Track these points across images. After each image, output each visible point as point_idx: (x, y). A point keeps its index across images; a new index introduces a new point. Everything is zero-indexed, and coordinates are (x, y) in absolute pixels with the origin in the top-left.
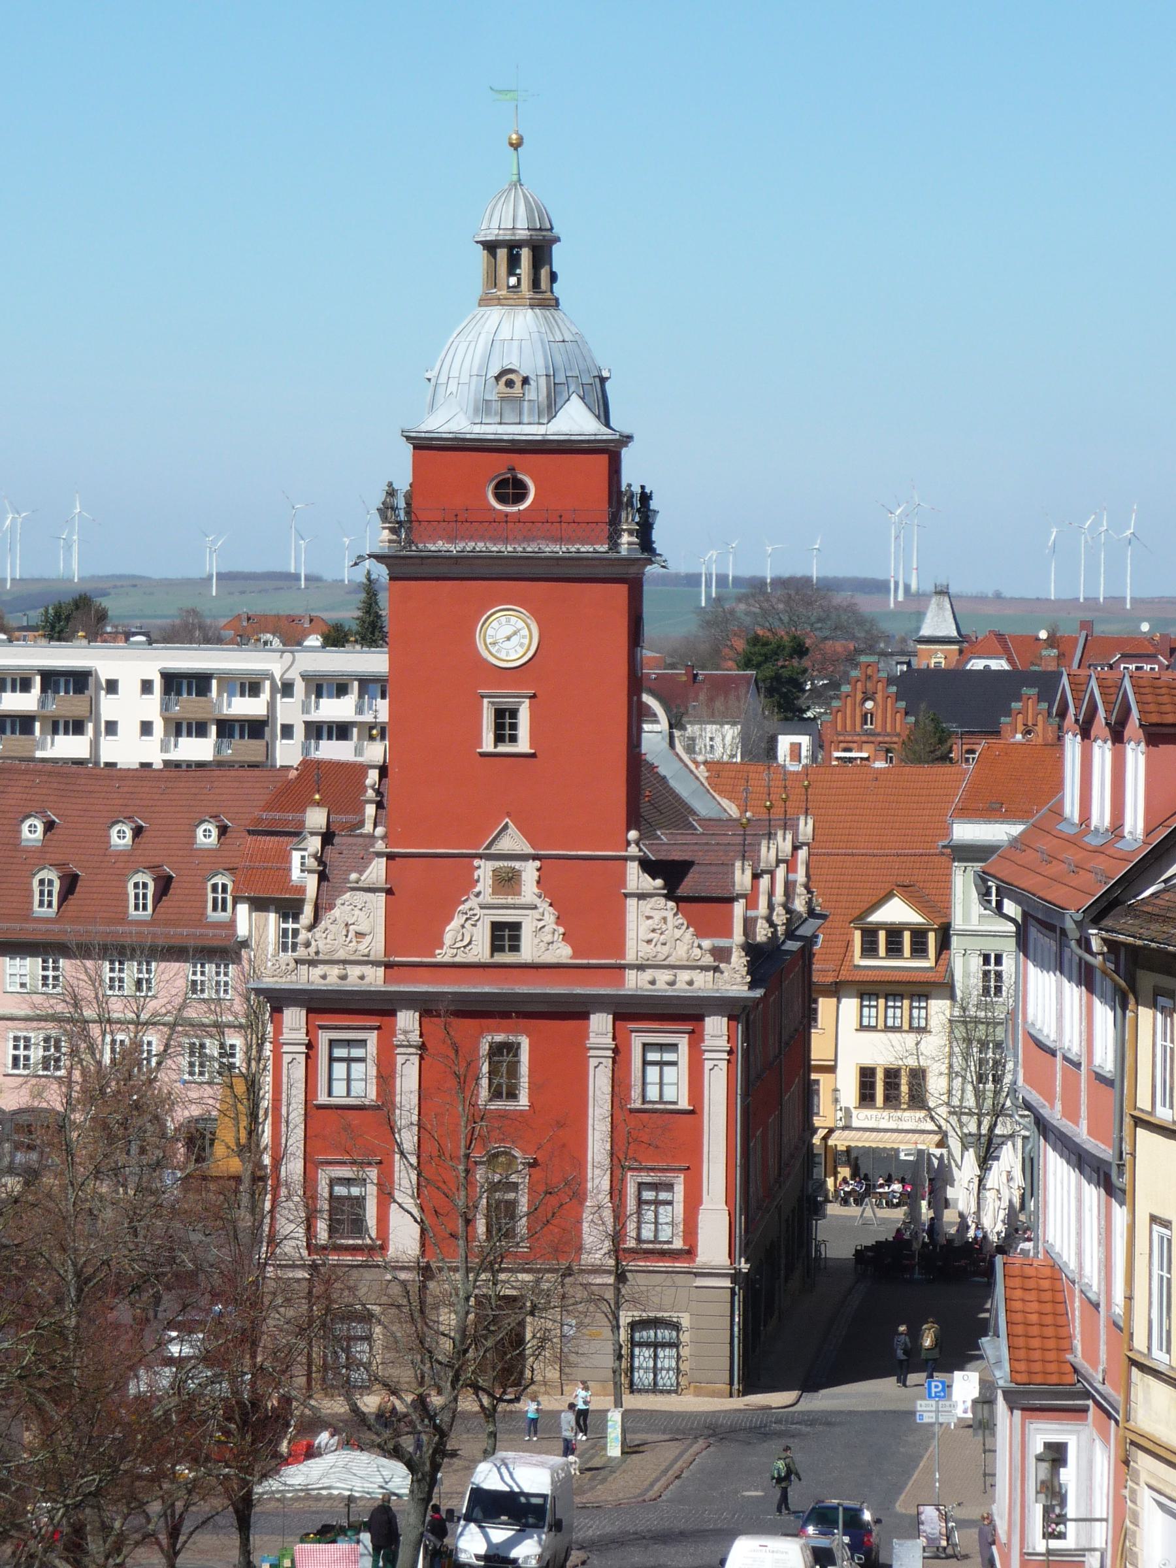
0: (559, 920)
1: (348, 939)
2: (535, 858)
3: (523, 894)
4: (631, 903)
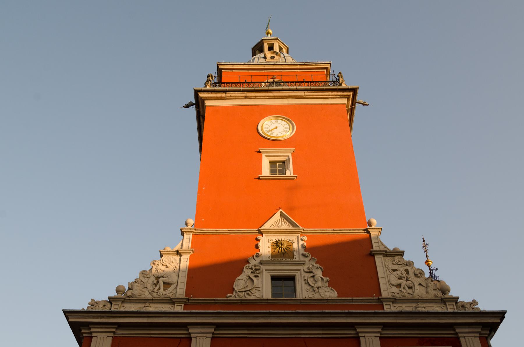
1: (158, 287)
3: (295, 257)
4: (379, 260)
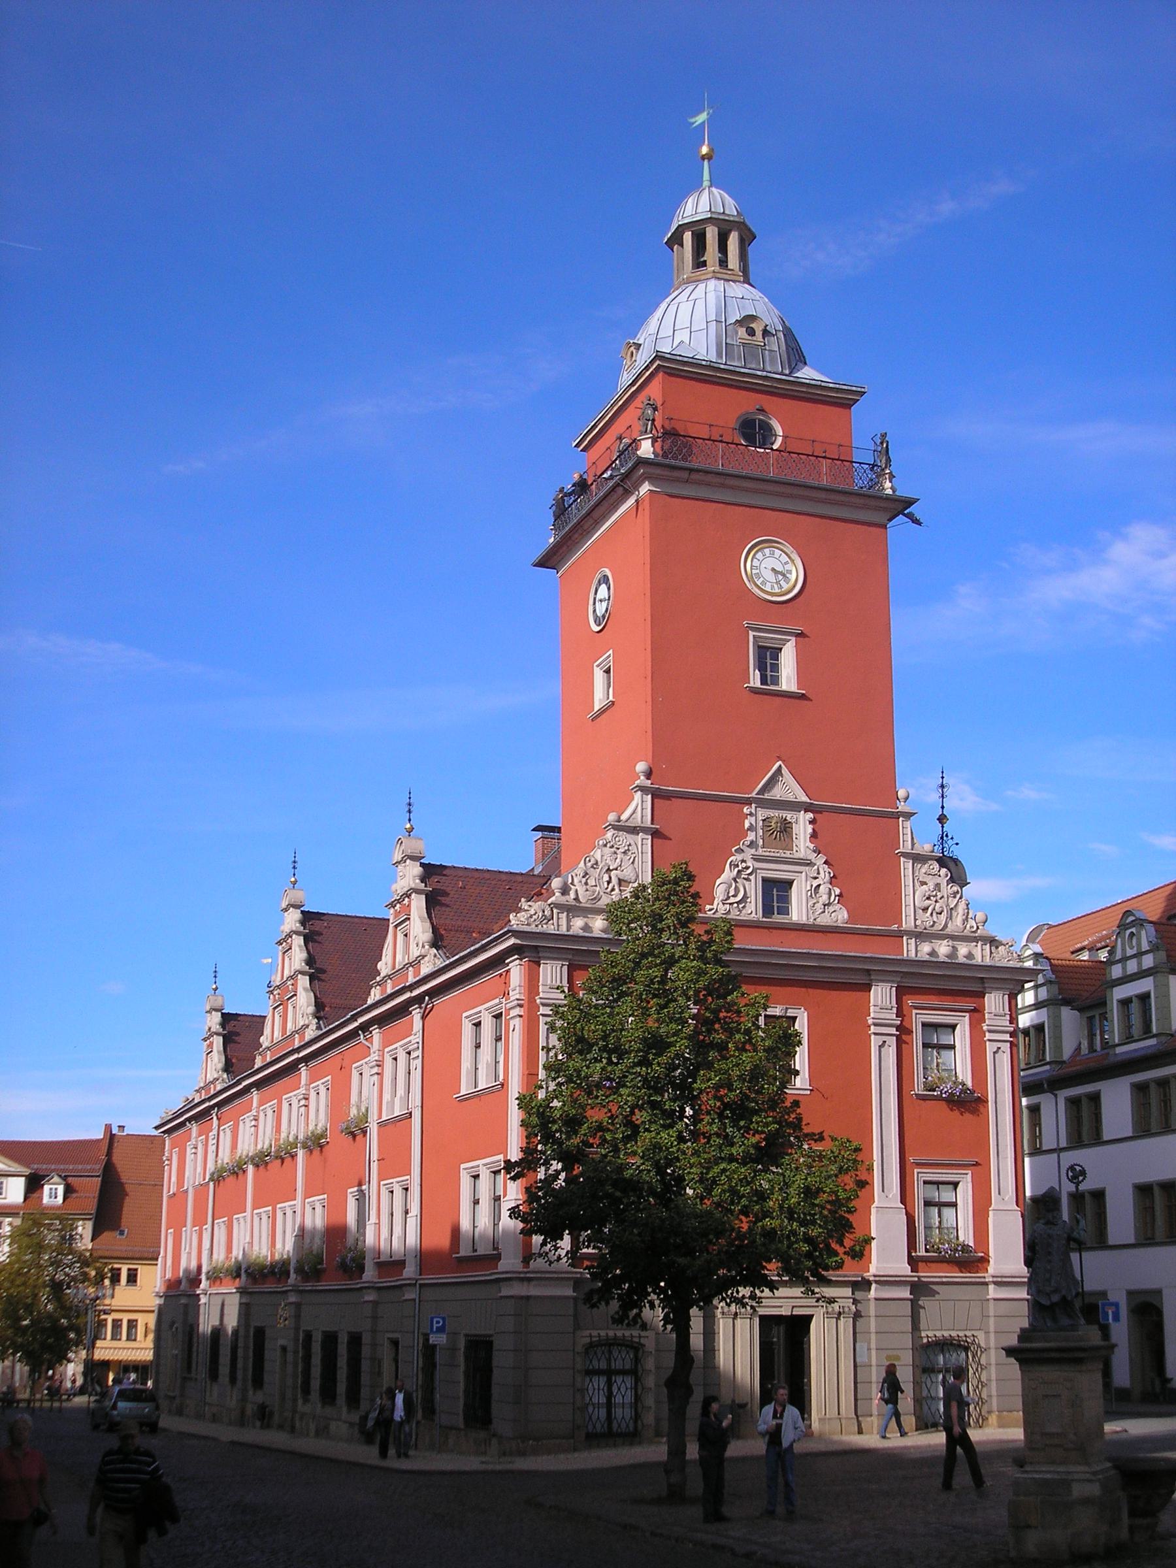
0: (833, 880)
2: (808, 808)
4: (906, 866)
